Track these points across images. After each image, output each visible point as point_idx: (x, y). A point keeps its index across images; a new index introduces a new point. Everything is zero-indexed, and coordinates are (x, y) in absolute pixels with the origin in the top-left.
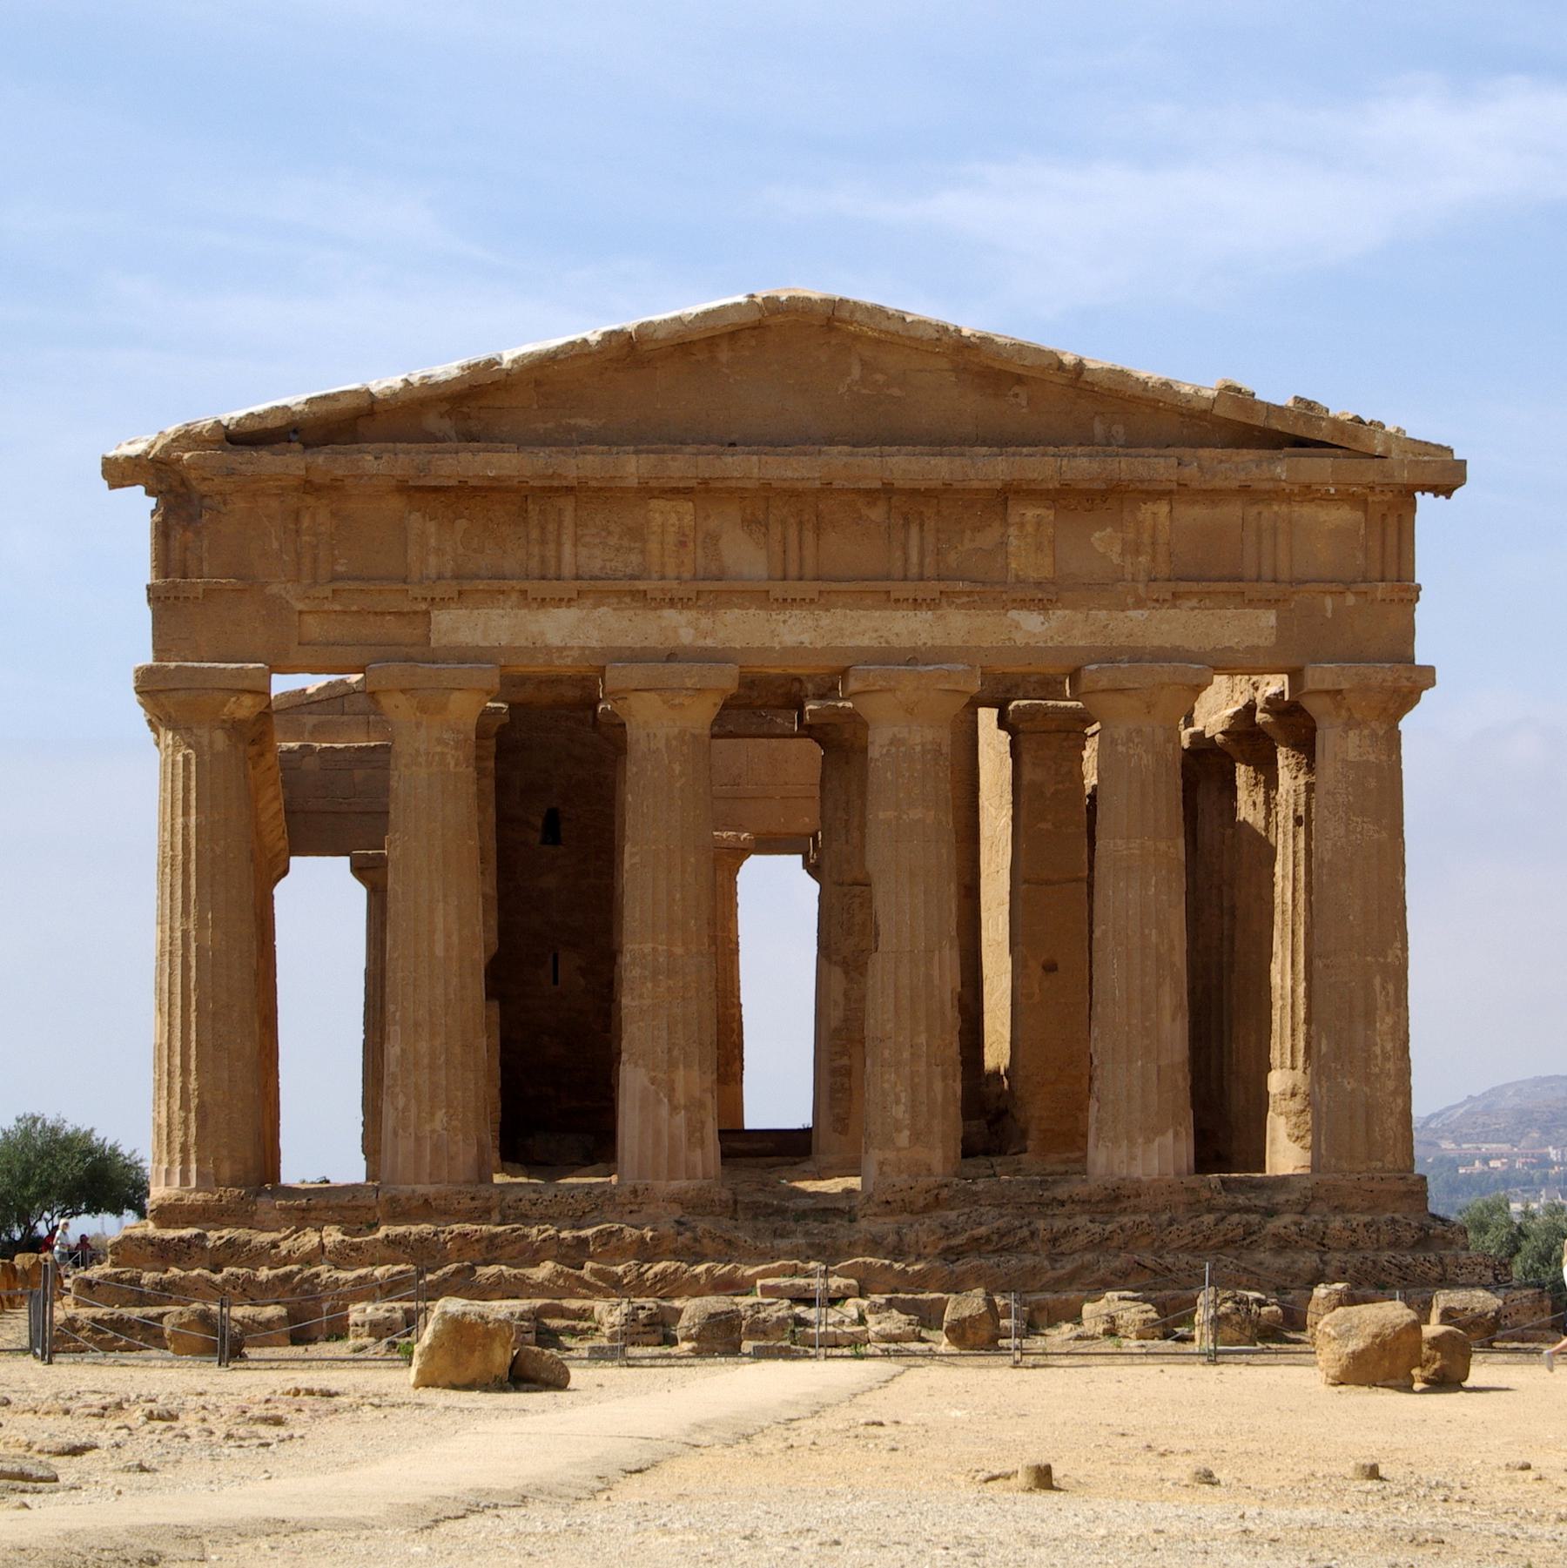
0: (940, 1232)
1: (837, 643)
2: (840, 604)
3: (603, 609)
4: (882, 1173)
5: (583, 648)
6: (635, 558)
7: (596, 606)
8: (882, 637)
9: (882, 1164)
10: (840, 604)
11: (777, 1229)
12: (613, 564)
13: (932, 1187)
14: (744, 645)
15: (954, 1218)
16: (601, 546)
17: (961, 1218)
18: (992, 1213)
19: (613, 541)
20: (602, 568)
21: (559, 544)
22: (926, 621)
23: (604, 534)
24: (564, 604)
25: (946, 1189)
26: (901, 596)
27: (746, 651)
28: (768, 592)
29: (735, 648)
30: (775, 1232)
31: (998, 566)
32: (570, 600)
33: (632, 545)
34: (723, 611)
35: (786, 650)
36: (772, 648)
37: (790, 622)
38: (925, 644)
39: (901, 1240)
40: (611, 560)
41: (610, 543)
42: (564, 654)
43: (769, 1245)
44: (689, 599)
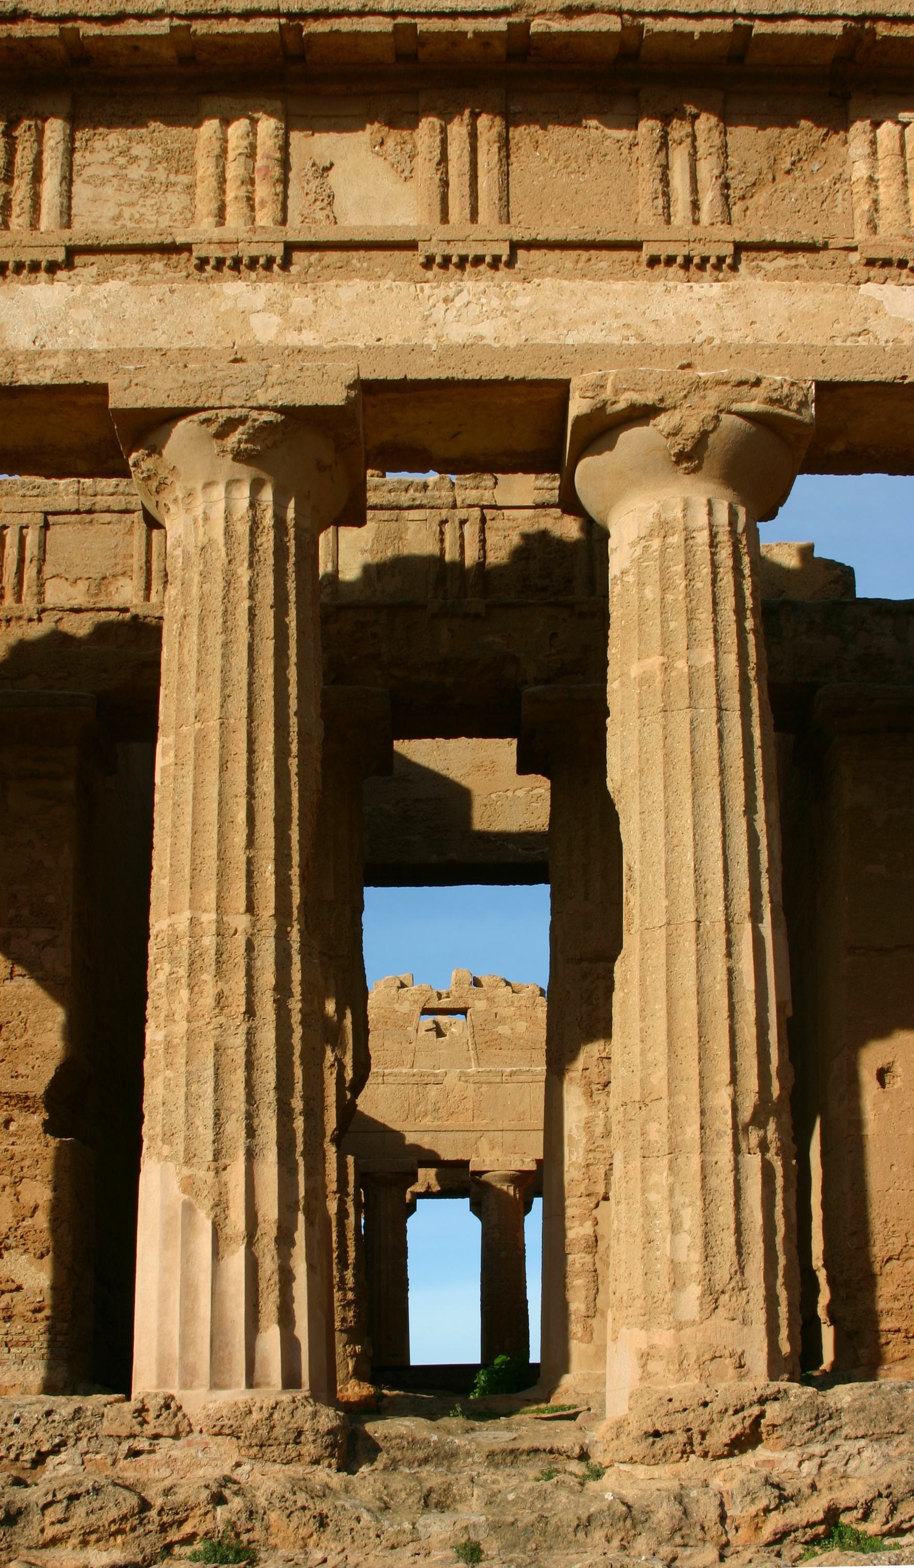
0: (767, 1498)
1: (547, 337)
2: (550, 270)
3: (113, 285)
4: (645, 1376)
5: (73, 353)
6: (176, 200)
7: (102, 278)
8: (627, 326)
9: (645, 1357)
10: (550, 270)
11: (430, 1491)
12: (135, 211)
13: (747, 1401)
14: (372, 342)
15: (793, 1465)
16: (115, 181)
17: (806, 1465)
18: (866, 1454)
19: (136, 172)
20: (118, 217)
21: (37, 178)
22: (710, 300)
23: (121, 161)
24: (43, 275)
25: (777, 1405)
26: (664, 251)
27: (377, 351)
28: (412, 246)
29: (355, 349)
30: (427, 1497)
31: (839, 210)
32: (53, 268)
33: (172, 178)
34: (333, 283)
35: (449, 351)
36: (425, 350)
37: (459, 301)
38: (710, 340)
39: (685, 1512)
40: (132, 204)
41: (131, 176)
42: (39, 363)
43: (407, 1526)
44: (270, 261)
